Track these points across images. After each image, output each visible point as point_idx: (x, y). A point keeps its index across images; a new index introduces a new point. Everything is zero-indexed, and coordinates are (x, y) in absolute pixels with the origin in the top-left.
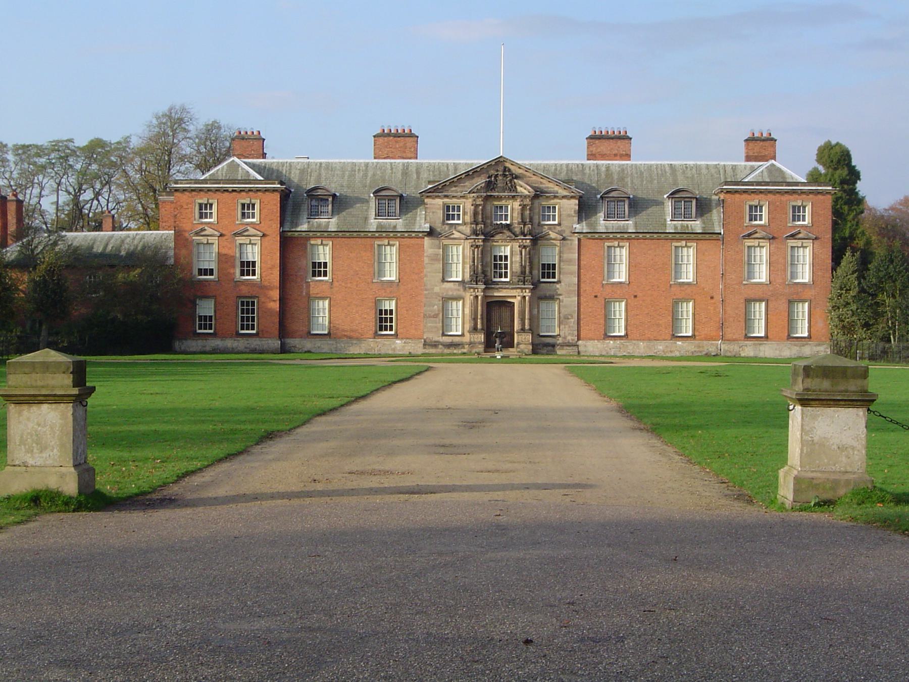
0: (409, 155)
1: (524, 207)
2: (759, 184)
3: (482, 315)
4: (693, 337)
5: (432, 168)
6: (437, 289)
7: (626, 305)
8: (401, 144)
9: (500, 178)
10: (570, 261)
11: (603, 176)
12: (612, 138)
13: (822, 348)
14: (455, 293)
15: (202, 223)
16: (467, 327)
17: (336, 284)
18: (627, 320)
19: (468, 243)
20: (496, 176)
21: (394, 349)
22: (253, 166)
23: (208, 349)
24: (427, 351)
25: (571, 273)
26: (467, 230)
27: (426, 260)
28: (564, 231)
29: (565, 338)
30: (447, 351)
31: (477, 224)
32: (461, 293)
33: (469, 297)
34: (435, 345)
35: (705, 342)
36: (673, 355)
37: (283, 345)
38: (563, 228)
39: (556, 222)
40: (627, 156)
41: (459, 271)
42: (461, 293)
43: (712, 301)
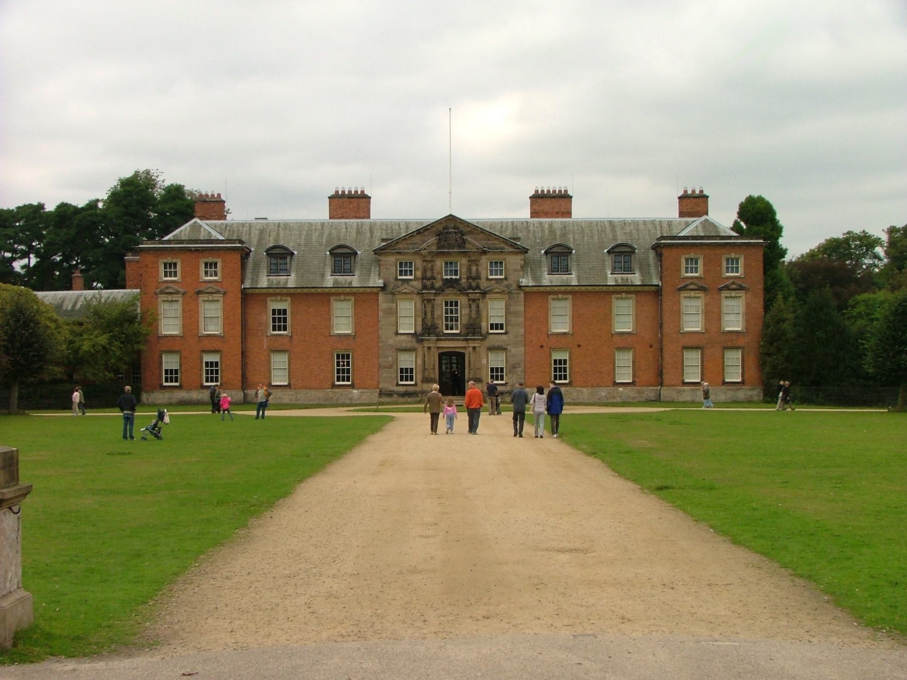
0: (362, 215)
2: (694, 238)
4: (633, 384)
5: (387, 226)
6: (391, 341)
8: (355, 205)
10: (516, 314)
11: (547, 232)
12: (554, 197)
13: (755, 392)
14: (409, 345)
15: (167, 282)
17: (295, 337)
21: (351, 399)
22: (215, 227)
23: (174, 401)
24: (382, 400)
26: (418, 285)
27: (381, 314)
28: (511, 285)
29: (513, 386)
30: (401, 400)
34: (390, 394)
35: (645, 388)
36: (615, 401)
37: (245, 395)
39: (503, 277)
40: (568, 214)
42: (414, 344)
43: (651, 349)
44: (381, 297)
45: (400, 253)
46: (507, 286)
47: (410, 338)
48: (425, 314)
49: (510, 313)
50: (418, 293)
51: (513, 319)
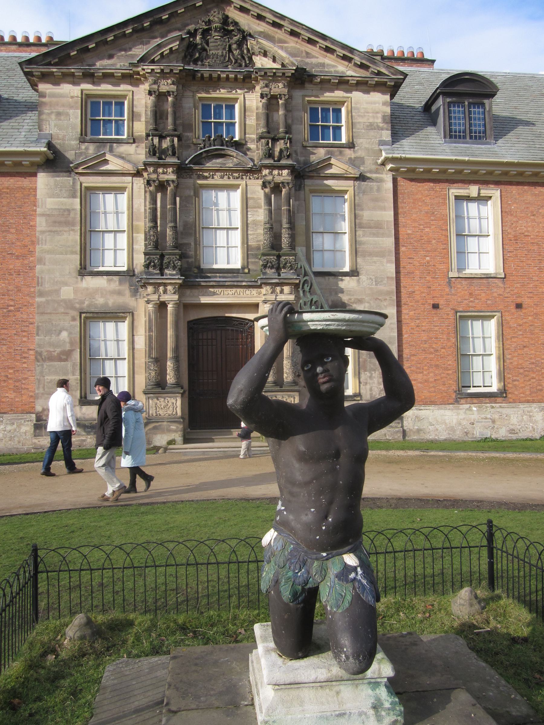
1: (271, 102)
3: (176, 349)
6: (67, 293)
7: (501, 325)
9: (216, 35)
10: (376, 227)
14: (112, 302)
16: (141, 381)
18: (502, 359)
19: (139, 183)
20: (206, 33)
25: (381, 254)
27: (41, 223)
28: (362, 160)
31: (162, 137)
32: (127, 300)
33: (143, 310)
38: (359, 152)
39: (344, 141)
41: (120, 248)
42: (127, 300)
44: (43, 180)
46: (352, 162)
47: (115, 283)
49: (361, 227)
50: (138, 174)
51: (367, 240)
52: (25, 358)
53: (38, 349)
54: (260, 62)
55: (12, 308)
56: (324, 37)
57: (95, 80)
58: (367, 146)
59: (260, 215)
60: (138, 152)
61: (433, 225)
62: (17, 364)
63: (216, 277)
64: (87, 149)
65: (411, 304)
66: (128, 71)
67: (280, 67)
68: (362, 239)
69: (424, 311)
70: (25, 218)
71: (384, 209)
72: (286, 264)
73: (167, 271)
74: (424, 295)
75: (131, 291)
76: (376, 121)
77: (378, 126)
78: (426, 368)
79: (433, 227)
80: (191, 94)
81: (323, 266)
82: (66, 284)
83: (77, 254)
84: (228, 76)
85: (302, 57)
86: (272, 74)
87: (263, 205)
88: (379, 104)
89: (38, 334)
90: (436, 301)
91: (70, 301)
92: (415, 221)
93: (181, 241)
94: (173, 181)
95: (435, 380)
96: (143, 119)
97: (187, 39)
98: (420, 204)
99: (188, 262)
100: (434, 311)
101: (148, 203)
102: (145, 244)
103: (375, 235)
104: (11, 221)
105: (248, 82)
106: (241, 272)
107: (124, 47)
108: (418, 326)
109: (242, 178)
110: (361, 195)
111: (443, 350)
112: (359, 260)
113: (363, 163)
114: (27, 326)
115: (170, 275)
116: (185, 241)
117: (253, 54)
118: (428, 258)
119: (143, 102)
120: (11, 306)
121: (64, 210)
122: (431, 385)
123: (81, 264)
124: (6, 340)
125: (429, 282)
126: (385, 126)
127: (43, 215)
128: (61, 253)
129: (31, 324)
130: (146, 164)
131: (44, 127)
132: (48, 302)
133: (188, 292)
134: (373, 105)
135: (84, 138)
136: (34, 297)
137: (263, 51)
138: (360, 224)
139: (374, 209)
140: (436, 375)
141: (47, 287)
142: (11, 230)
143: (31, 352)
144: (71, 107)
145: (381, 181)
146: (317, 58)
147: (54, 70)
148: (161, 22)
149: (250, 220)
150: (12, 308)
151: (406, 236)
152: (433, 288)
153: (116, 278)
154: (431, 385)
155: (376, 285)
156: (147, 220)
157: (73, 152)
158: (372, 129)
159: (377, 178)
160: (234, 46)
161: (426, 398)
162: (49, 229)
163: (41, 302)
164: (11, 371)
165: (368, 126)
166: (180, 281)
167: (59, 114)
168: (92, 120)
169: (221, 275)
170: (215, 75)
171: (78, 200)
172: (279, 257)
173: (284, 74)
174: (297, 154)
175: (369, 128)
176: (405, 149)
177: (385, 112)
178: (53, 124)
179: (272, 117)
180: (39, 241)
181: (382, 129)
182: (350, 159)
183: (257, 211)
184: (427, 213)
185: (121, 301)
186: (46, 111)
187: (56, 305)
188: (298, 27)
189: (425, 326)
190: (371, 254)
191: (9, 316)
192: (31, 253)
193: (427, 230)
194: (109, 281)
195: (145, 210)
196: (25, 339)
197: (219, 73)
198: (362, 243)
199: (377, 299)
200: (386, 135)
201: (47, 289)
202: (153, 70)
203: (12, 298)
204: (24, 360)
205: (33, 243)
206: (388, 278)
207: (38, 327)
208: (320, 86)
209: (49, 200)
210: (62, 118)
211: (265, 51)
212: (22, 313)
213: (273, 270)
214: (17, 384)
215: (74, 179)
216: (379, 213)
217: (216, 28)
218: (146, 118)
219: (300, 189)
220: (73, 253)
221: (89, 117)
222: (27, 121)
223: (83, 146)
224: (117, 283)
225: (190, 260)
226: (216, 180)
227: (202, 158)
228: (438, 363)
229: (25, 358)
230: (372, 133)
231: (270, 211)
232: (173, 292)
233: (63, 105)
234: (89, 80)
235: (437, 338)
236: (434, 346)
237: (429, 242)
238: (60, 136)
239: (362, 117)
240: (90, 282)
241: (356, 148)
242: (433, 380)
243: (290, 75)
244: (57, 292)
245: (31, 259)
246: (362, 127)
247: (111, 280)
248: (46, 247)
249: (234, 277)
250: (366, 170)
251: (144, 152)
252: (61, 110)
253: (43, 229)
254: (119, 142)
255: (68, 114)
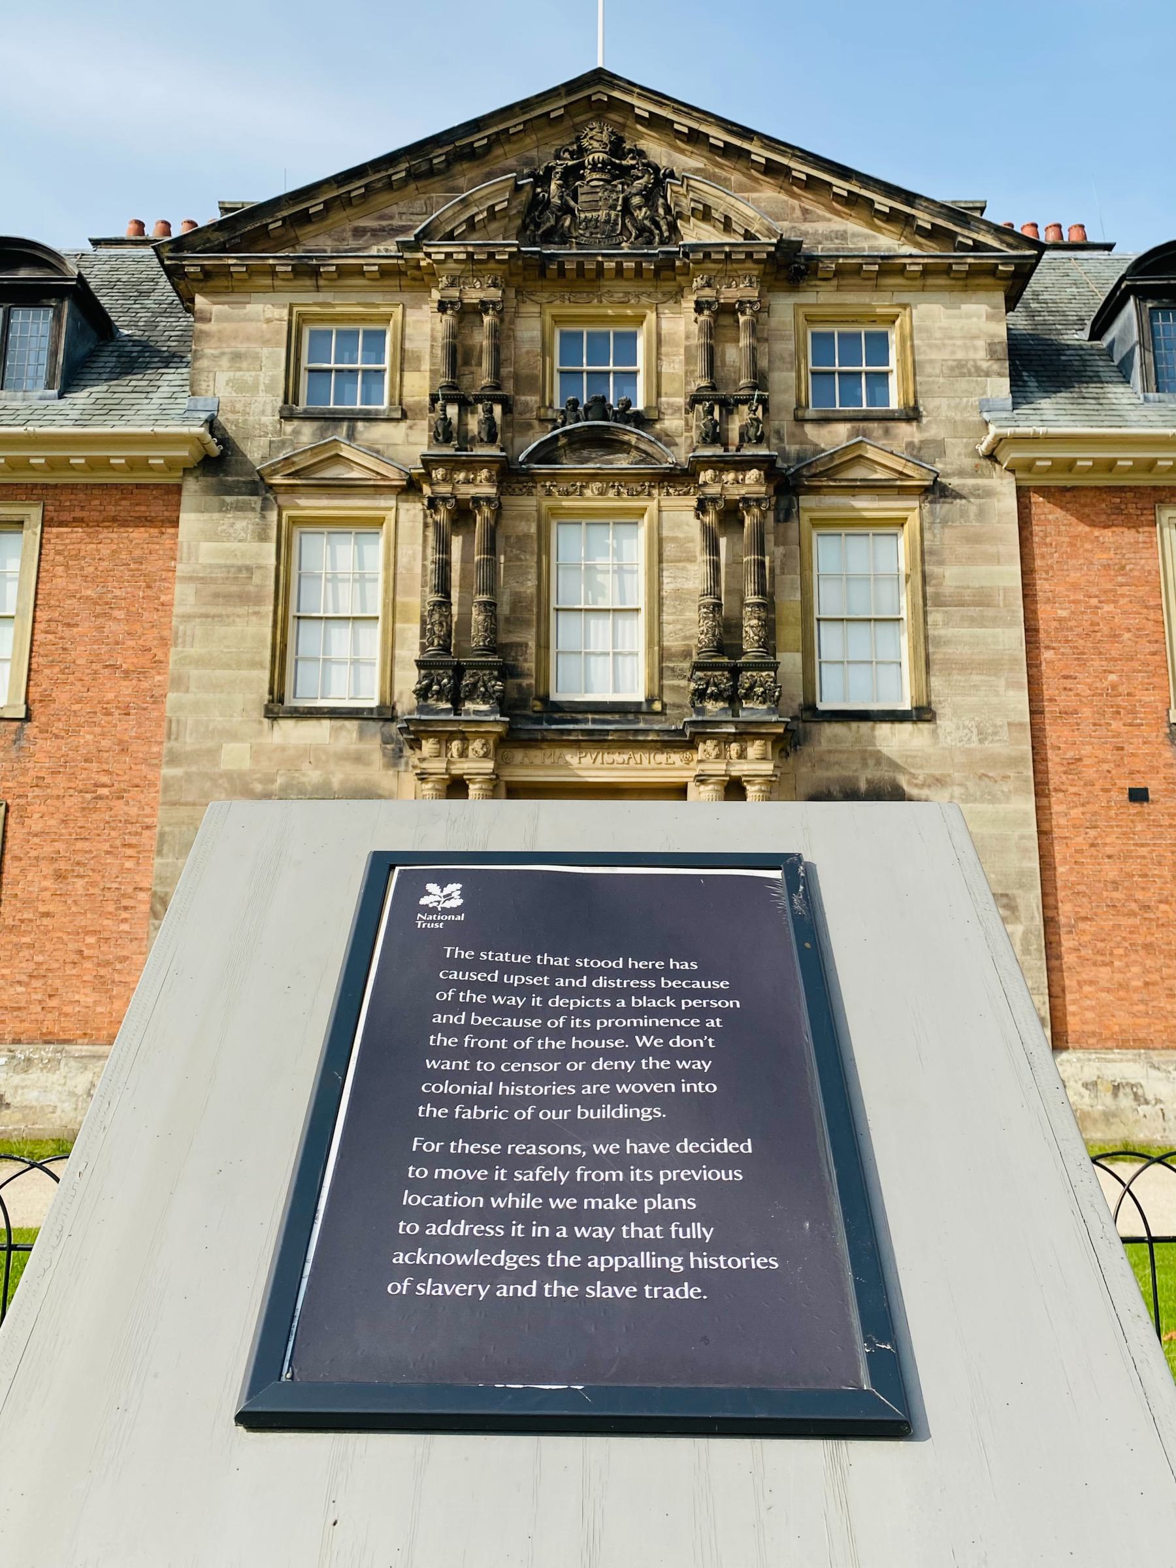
1: (718, 318)
6: (235, 757)
9: (594, 178)
19: (412, 512)
20: (572, 175)
25: (992, 666)
27: (184, 598)
28: (940, 448)
31: (465, 405)
45: (307, 272)
46: (916, 453)
48: (443, 586)
49: (939, 604)
50: (410, 487)
52: (126, 908)
53: (159, 889)
54: (695, 233)
55: (105, 791)
56: (845, 173)
57: (321, 282)
58: (951, 414)
59: (691, 577)
60: (412, 439)
61: (1123, 596)
62: (106, 922)
63: (586, 721)
64: (296, 433)
65: (1072, 790)
66: (395, 261)
67: (741, 240)
68: (942, 632)
69: (1109, 807)
70: (149, 587)
71: (997, 559)
72: (752, 687)
73: (469, 706)
74: (1106, 767)
75: (384, 755)
76: (972, 355)
77: (978, 369)
78: (1121, 951)
79: (1122, 601)
80: (537, 309)
81: (845, 700)
82: (234, 736)
83: (263, 667)
84: (619, 264)
85: (792, 220)
86: (722, 256)
87: (698, 554)
88: (979, 317)
89: (160, 853)
90: (1139, 784)
91: (241, 775)
92: (1075, 587)
93: (504, 638)
94: (488, 500)
95: (1147, 984)
96: (426, 366)
97: (528, 188)
98: (1088, 546)
99: (520, 686)
100: (1135, 808)
101: (429, 551)
102: (422, 644)
103: (973, 621)
104: (118, 592)
105: (665, 280)
106: (644, 708)
107: (387, 211)
108: (1092, 845)
109: (650, 494)
110: (937, 529)
111: (1163, 907)
112: (935, 682)
113: (942, 453)
114: (136, 834)
115: (476, 712)
116: (515, 638)
117: (680, 215)
118: (1113, 677)
119: (427, 328)
120: (104, 786)
121: (240, 569)
122: (1136, 997)
123: (271, 692)
124: (84, 865)
125: (1118, 735)
126: (996, 367)
127: (190, 579)
128: (227, 666)
129: (148, 827)
130: (428, 463)
131: (204, 385)
132: (188, 777)
133: (518, 755)
134: (964, 321)
135: (291, 409)
136: (158, 766)
137: (701, 207)
138: (937, 595)
139: (971, 559)
140: (1146, 971)
141: (189, 742)
142: (117, 613)
143: (142, 896)
144: (266, 342)
145: (988, 493)
146: (829, 220)
147: (231, 262)
148: (471, 155)
149: (668, 587)
150: (105, 791)
151: (1055, 624)
152: (1129, 749)
153: (352, 725)
154: (1136, 997)
155: (981, 741)
156: (427, 589)
157: (264, 441)
158: (963, 375)
159: (977, 488)
160: (636, 200)
161: (1122, 1031)
162: (203, 610)
163: (173, 777)
164: (91, 940)
165: (952, 369)
166: (499, 729)
167: (237, 357)
168: (311, 371)
169: (597, 717)
170: (590, 266)
171: (272, 546)
172: (735, 672)
173: (749, 255)
174: (781, 439)
175: (957, 372)
176: (1044, 418)
177: (993, 336)
178: (222, 377)
179: (724, 353)
180: (177, 638)
181: (988, 374)
182: (910, 445)
183: (684, 569)
184: (1107, 567)
185: (362, 777)
186: (208, 351)
187: (208, 784)
188: (783, 153)
189: (1112, 844)
190: (965, 667)
191: (96, 810)
192: (159, 664)
193: (1108, 608)
194: (335, 732)
195: (424, 566)
196: (129, 864)
197: (600, 259)
198: (939, 642)
199: (982, 777)
200: (1000, 387)
201: (188, 748)
202: (449, 255)
203: (105, 767)
204: (124, 915)
205: (164, 642)
206: (1009, 724)
207: (162, 835)
208: (834, 282)
209: (205, 546)
210: (244, 365)
211: (705, 206)
212: (127, 803)
213: (721, 704)
214: (103, 971)
215: (265, 499)
216: (983, 569)
217: (594, 164)
218: (433, 364)
219: (787, 518)
220: (255, 664)
221: (305, 363)
222: (170, 377)
223: (289, 427)
224: (355, 735)
225: (525, 682)
226: (588, 499)
227: (559, 448)
228: (1149, 939)
229: (126, 908)
230: (963, 384)
231: (715, 566)
232: (481, 753)
233: (248, 339)
234: (309, 282)
235: (1146, 876)
236: (1139, 895)
237: (1114, 637)
238: (239, 407)
239: (938, 348)
240: (291, 732)
241: (924, 420)
242: (1139, 983)
243: (765, 256)
244: (213, 754)
245: (158, 678)
246: (938, 371)
247: (341, 728)
248: (195, 651)
249: (629, 722)
250: (949, 469)
251: (426, 440)
252: (242, 347)
253: (188, 610)
254: (370, 418)
255: (256, 357)
